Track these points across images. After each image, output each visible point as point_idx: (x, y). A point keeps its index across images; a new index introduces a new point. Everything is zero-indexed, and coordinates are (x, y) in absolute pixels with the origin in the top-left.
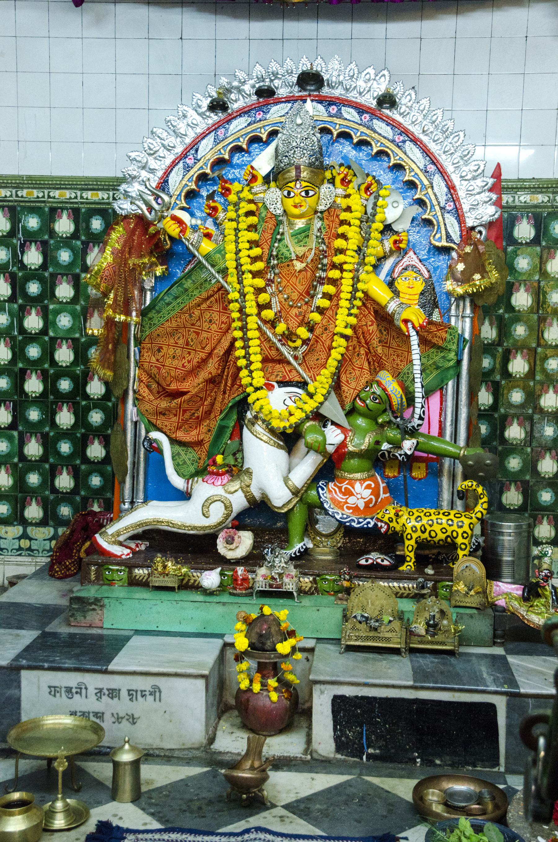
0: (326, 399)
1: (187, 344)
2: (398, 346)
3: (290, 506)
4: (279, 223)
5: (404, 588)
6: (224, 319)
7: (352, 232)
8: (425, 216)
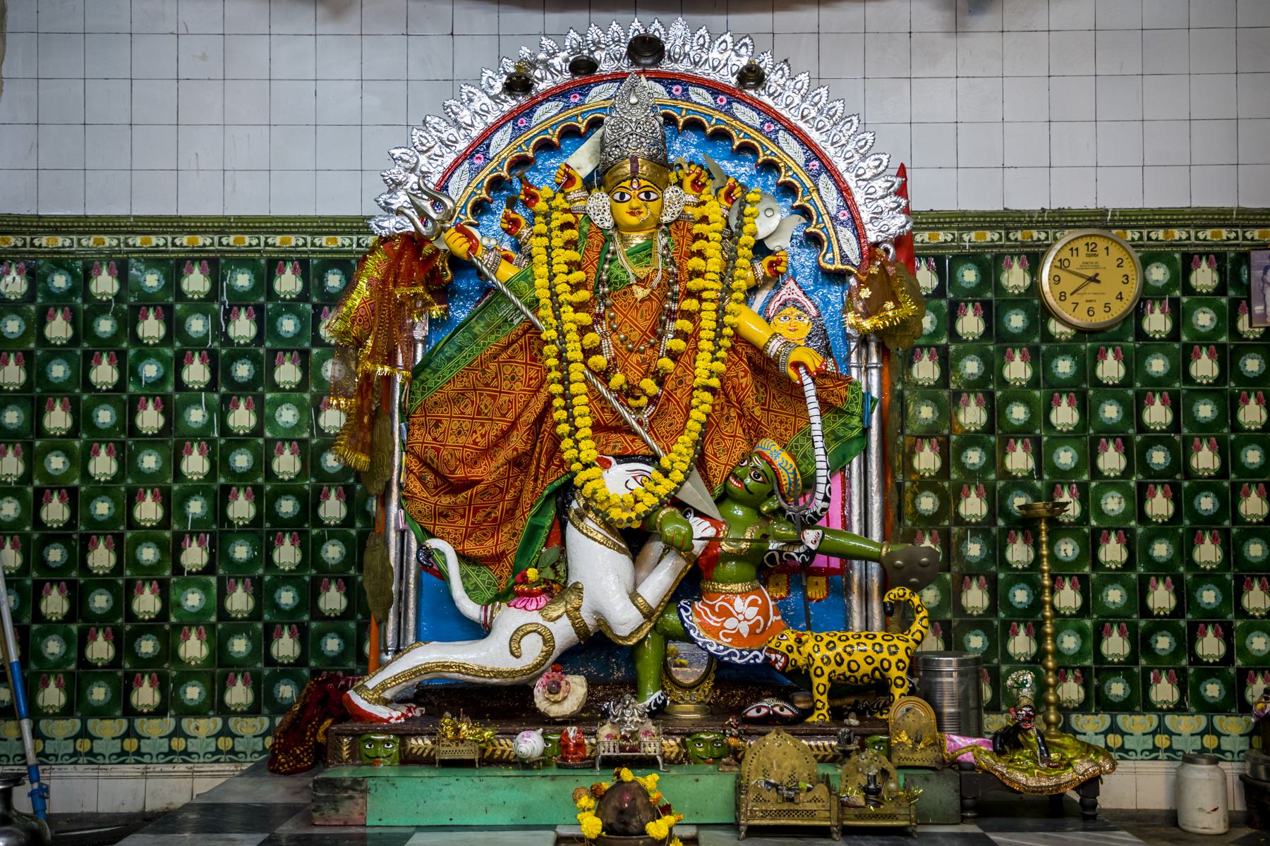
0: (687, 478)
1: (479, 413)
2: (782, 408)
3: (641, 635)
4: (608, 239)
5: (817, 747)
6: (533, 374)
7: (712, 249)
8: (811, 229)
